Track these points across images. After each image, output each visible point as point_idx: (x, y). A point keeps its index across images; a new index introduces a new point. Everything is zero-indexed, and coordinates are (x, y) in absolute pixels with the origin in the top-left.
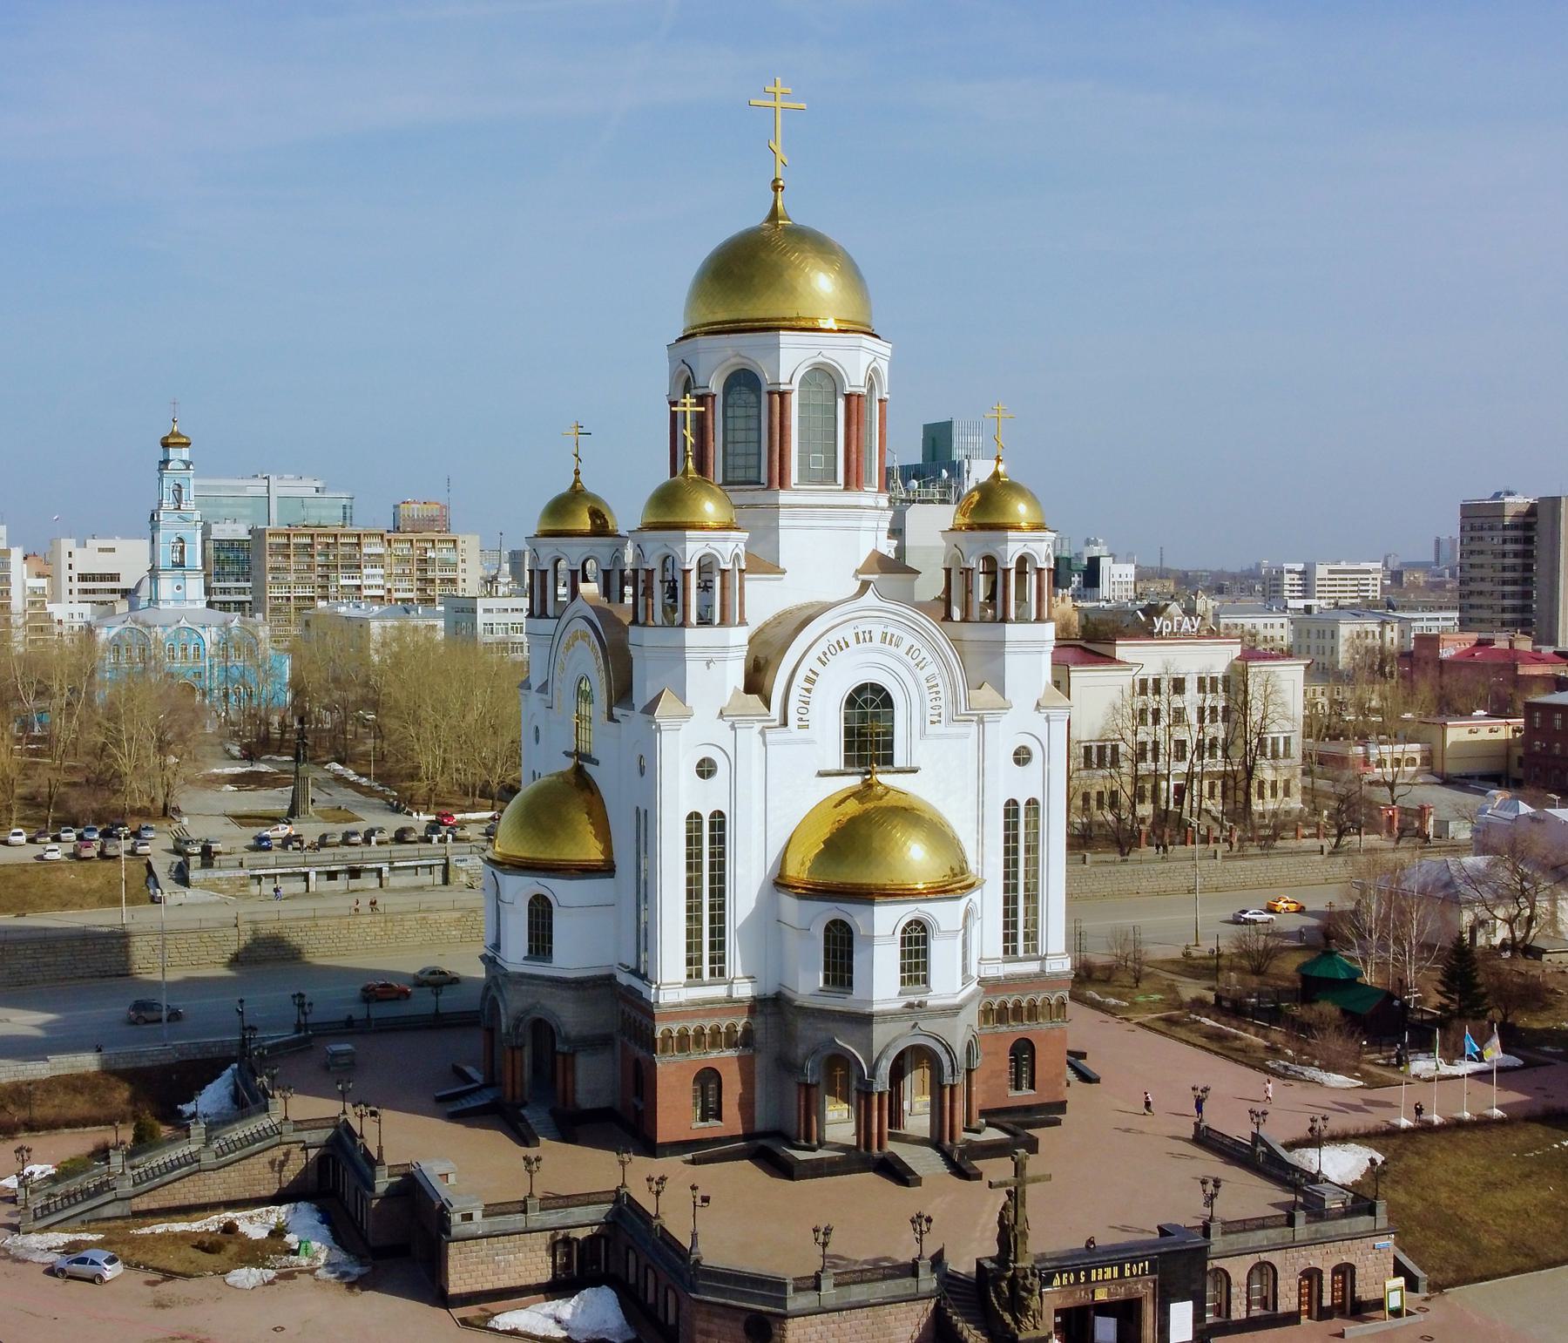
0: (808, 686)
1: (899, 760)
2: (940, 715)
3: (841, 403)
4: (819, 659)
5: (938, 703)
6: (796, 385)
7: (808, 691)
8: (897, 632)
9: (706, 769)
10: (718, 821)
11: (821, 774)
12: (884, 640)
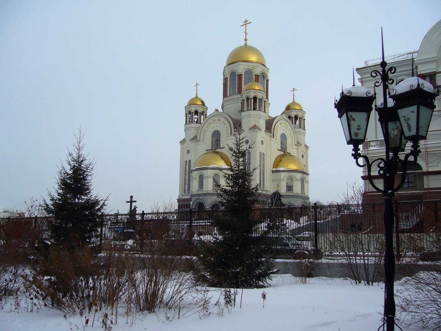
0: (204, 132)
1: (221, 146)
2: (228, 135)
3: (237, 76)
4: (206, 127)
5: (228, 132)
6: (228, 77)
7: (204, 133)
8: (221, 119)
9: (188, 152)
10: (190, 161)
11: (207, 150)
12: (218, 121)
